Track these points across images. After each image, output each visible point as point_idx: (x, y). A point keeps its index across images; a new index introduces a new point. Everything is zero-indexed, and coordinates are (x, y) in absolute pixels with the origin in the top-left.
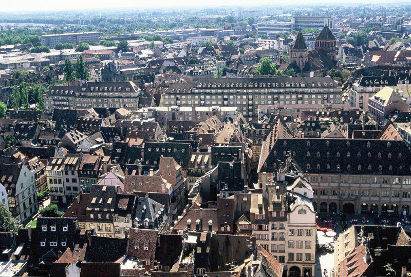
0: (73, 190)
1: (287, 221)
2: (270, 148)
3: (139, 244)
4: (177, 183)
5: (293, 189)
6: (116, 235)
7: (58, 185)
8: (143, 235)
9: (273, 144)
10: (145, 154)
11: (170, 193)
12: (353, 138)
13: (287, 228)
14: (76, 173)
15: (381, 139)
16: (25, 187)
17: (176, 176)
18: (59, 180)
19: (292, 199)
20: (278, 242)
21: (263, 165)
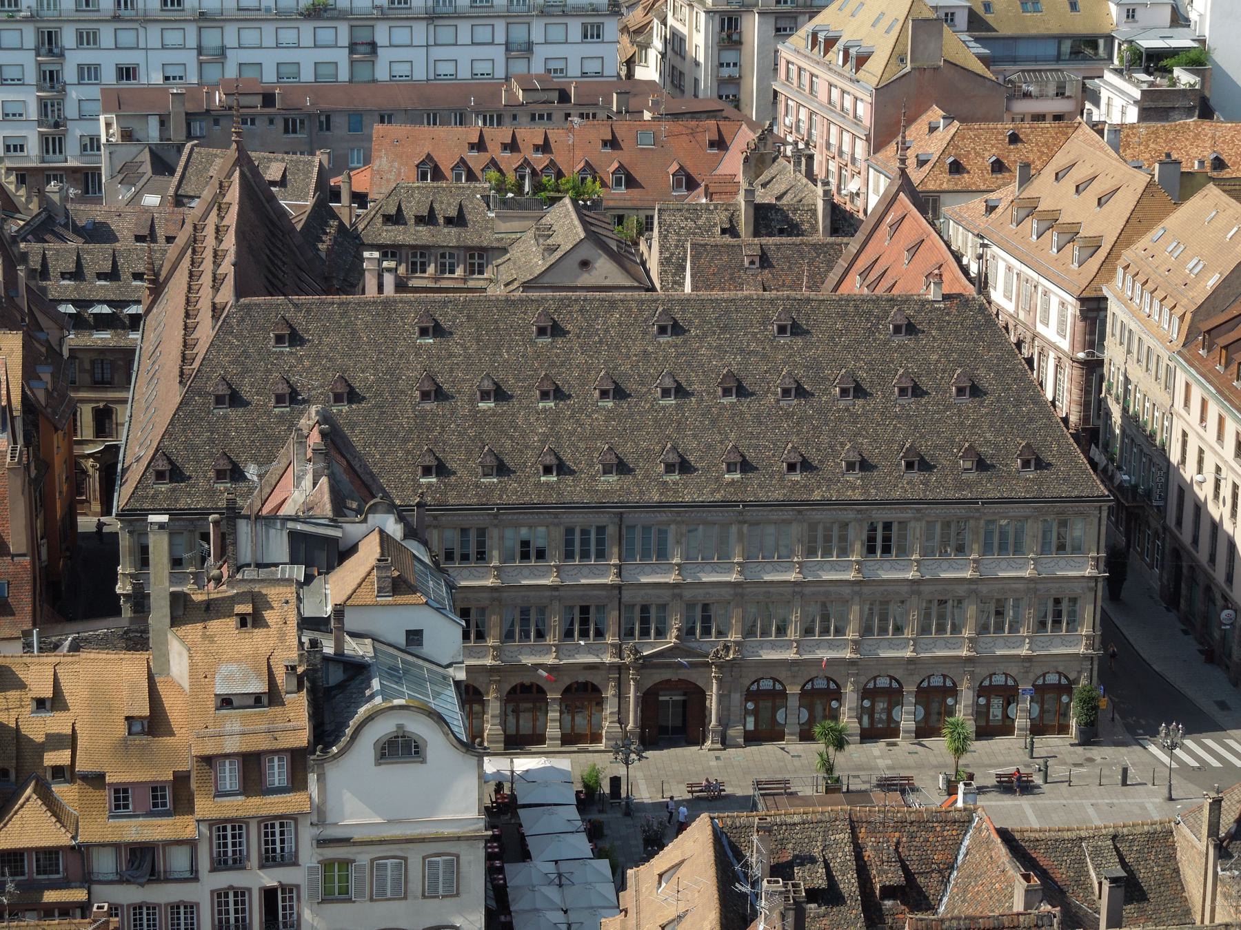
5: (339, 611)
9: (205, 331)
12: (688, 288)
13: (309, 856)
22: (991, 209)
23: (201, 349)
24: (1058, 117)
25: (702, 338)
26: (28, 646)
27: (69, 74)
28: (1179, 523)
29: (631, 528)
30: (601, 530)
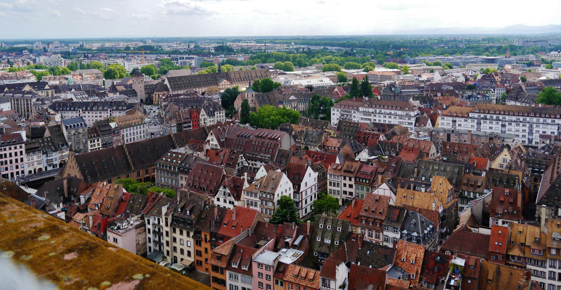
0: (349, 195)
2: (551, 180)
3: (407, 256)
4: (448, 203)
6: (385, 244)
7: (336, 189)
8: (410, 248)
9: (555, 176)
11: (440, 210)
14: (353, 179)
16: (309, 186)
17: (447, 195)
18: (338, 183)
21: (543, 198)
23: (554, 179)
26: (519, 222)
27: (534, 132)
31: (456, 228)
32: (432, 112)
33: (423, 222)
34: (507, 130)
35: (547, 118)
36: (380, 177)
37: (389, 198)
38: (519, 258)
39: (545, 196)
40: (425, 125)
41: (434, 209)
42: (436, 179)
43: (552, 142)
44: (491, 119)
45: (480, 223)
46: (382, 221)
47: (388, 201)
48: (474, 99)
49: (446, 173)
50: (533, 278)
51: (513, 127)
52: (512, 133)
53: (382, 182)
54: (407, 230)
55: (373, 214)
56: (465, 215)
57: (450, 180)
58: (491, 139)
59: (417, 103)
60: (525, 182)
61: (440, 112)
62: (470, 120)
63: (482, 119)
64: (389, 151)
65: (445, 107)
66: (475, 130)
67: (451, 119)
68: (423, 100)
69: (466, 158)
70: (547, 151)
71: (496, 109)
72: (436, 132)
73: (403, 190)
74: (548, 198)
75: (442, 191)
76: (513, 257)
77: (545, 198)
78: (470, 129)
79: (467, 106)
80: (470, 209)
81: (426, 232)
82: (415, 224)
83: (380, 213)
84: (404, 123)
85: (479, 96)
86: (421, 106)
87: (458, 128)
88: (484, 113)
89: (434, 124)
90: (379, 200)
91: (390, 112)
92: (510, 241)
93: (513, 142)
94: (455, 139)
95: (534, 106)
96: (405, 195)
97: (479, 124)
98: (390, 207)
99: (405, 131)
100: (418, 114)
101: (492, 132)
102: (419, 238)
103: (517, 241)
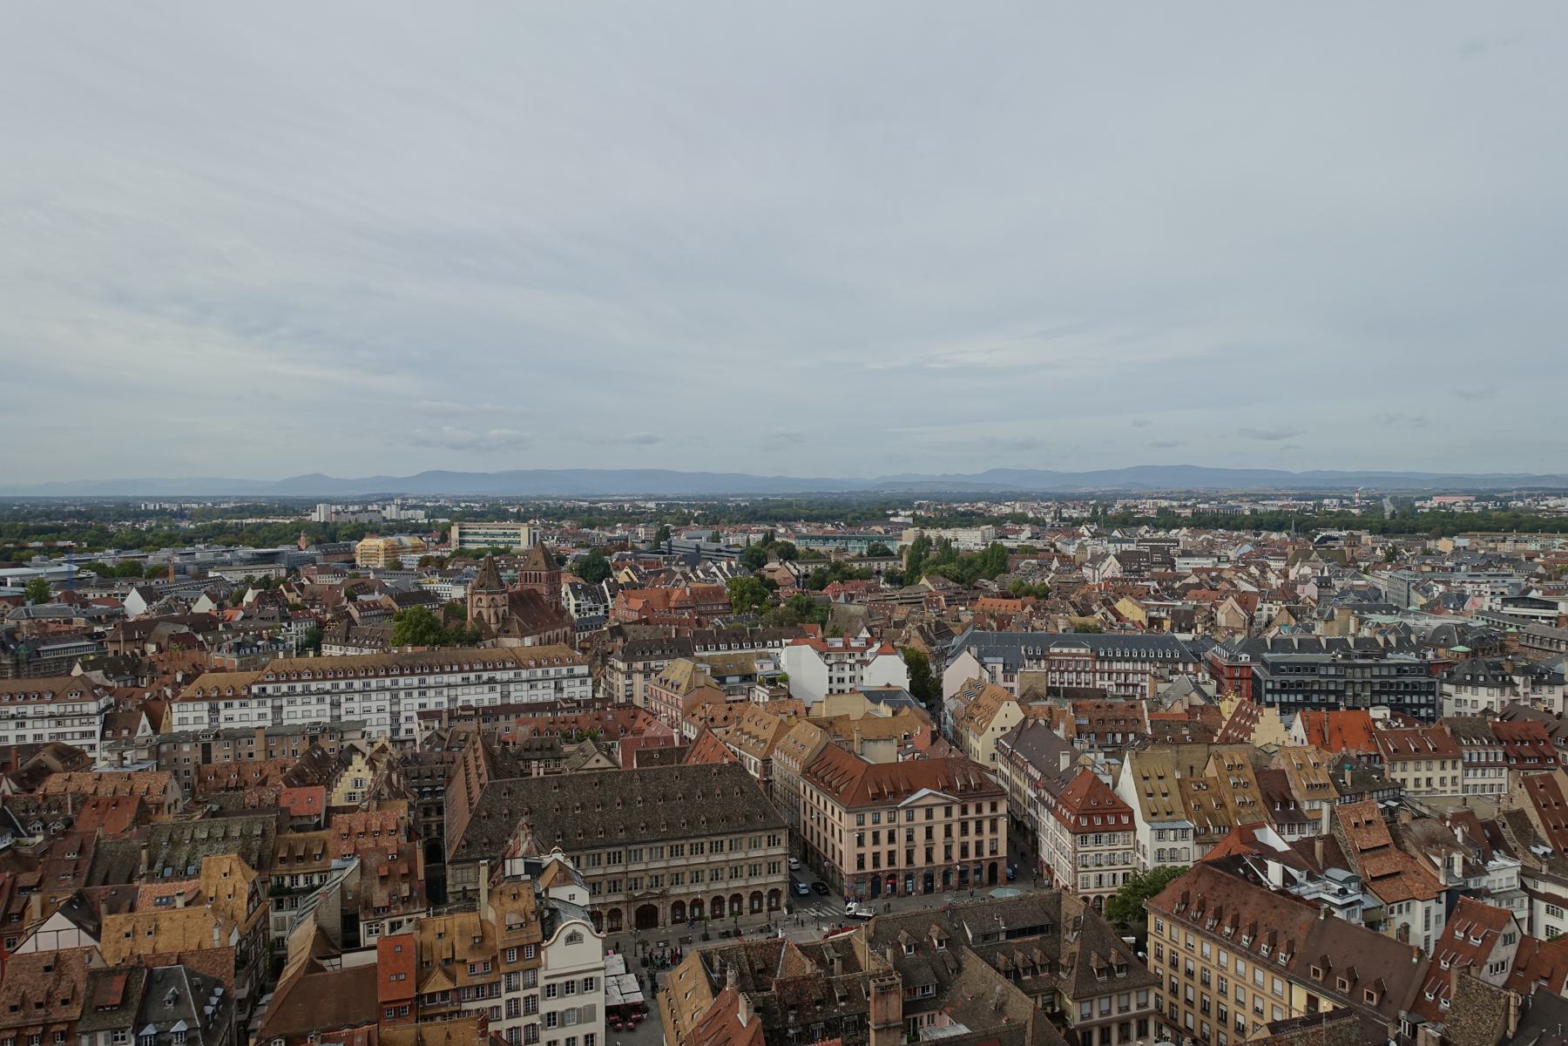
1: (540, 967)
2: (471, 804)
10: (149, 854)
13: (542, 983)
15: (693, 761)
17: (246, 896)
19: (546, 914)
20: (521, 1022)
22: (727, 733)
23: (476, 800)
24: (741, 701)
25: (650, 783)
26: (428, 915)
28: (805, 833)
29: (630, 851)
30: (620, 853)
31: (277, 977)
32: (147, 695)
33: (198, 987)
34: (343, 712)
35: (426, 674)
36: (36, 900)
37: (89, 952)
38: (445, 994)
39: (464, 843)
40: (132, 731)
41: (217, 945)
42: (212, 864)
43: (445, 725)
44: (307, 692)
45: (338, 943)
46: (71, 1023)
47: (87, 961)
48: (248, 651)
49: (231, 845)
50: (492, 1027)
51: (357, 704)
52: (356, 718)
53: (46, 914)
54: (155, 1023)
55: (42, 1011)
56: (300, 939)
57: (245, 856)
58: (313, 739)
59: (97, 676)
60: (412, 822)
61: (169, 692)
62: (254, 703)
63: (284, 695)
64: (41, 819)
65: (179, 678)
66: (269, 724)
67: (206, 705)
68: (114, 668)
69: (269, 796)
70: (436, 746)
71: (316, 668)
72: (171, 745)
73: (121, 917)
74: (469, 844)
75: (230, 891)
76: (432, 996)
77: (463, 847)
78: (256, 725)
79: (232, 671)
80: (312, 916)
81: (209, 1010)
82: (177, 1000)
83: (65, 1002)
84: (69, 736)
85: (260, 643)
86: (109, 684)
87: (223, 726)
88: (288, 680)
89: (155, 725)
90: (56, 964)
91: (21, 710)
92: (422, 962)
93: (363, 737)
94: (223, 754)
95: (396, 652)
96: (128, 929)
97: (277, 710)
98: (94, 975)
99: (72, 758)
100: (109, 706)
101: (315, 723)
102: (192, 1034)
103: (436, 957)
